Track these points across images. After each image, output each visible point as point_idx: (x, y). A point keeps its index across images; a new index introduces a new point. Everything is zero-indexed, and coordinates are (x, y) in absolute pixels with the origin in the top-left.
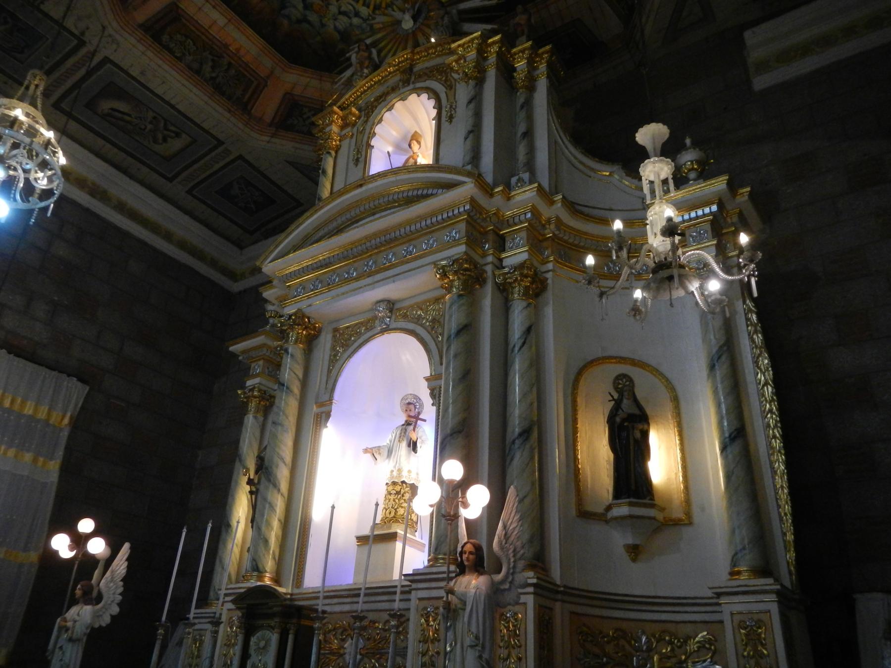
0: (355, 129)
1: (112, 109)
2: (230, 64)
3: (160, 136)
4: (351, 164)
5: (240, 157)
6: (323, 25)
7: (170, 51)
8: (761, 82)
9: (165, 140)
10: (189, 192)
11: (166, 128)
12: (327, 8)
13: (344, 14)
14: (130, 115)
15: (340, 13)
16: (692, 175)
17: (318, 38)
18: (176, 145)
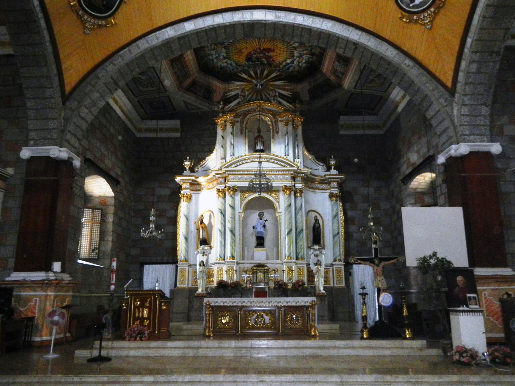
0: (239, 120)
1: (138, 77)
2: (185, 71)
3: (147, 86)
4: (239, 133)
5: (168, 97)
6: (217, 63)
7: (173, 67)
8: (342, 132)
9: (146, 87)
10: (138, 101)
11: (151, 85)
12: (223, 60)
13: (227, 63)
14: (142, 80)
15: (226, 62)
16: (333, 167)
17: (212, 65)
18: (149, 89)
